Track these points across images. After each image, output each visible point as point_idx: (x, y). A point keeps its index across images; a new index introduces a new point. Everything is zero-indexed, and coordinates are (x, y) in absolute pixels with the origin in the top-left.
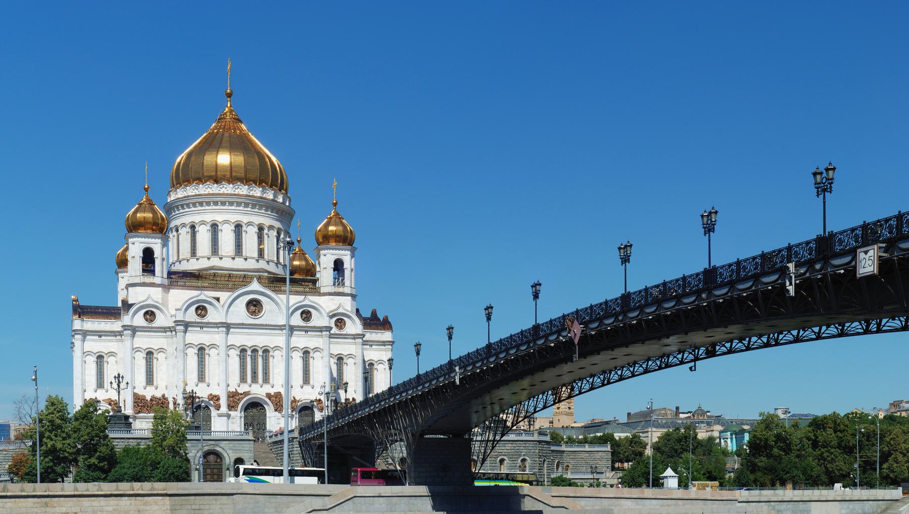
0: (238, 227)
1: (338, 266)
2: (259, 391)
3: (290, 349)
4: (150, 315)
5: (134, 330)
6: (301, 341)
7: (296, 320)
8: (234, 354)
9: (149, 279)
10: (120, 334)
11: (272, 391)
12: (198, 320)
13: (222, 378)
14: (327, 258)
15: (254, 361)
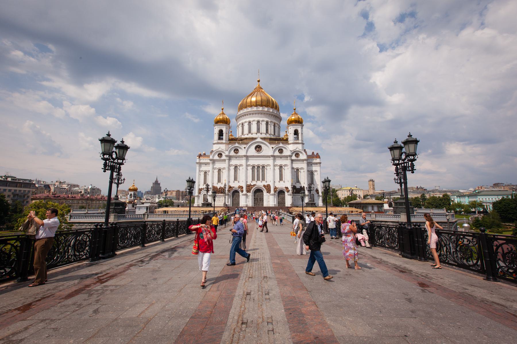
0: (258, 122)
1: (296, 133)
2: (260, 184)
3: (275, 166)
4: (220, 155)
5: (214, 161)
6: (279, 162)
7: (277, 153)
8: (250, 168)
9: (220, 141)
10: (208, 163)
11: (266, 184)
12: (235, 154)
13: (244, 178)
14: (291, 130)
15: (259, 171)
